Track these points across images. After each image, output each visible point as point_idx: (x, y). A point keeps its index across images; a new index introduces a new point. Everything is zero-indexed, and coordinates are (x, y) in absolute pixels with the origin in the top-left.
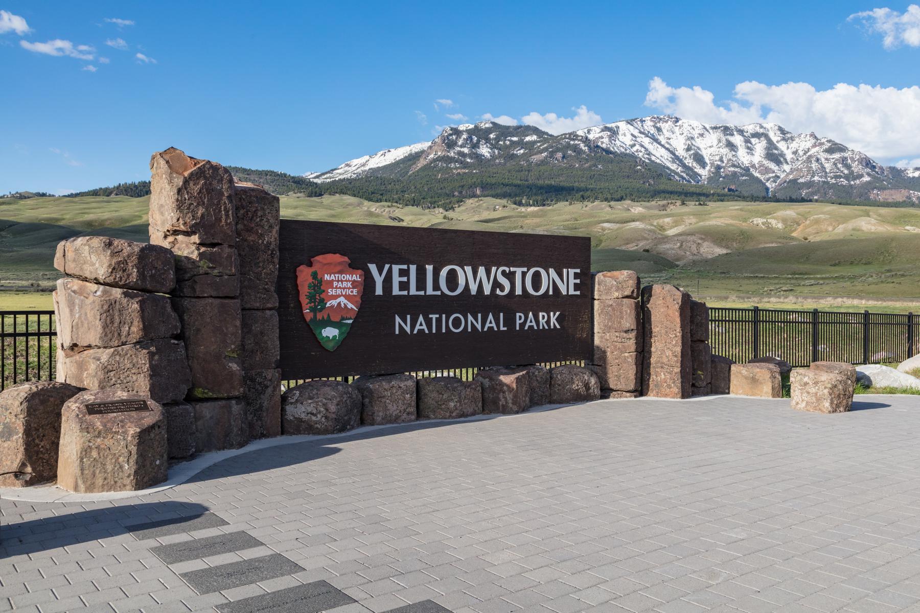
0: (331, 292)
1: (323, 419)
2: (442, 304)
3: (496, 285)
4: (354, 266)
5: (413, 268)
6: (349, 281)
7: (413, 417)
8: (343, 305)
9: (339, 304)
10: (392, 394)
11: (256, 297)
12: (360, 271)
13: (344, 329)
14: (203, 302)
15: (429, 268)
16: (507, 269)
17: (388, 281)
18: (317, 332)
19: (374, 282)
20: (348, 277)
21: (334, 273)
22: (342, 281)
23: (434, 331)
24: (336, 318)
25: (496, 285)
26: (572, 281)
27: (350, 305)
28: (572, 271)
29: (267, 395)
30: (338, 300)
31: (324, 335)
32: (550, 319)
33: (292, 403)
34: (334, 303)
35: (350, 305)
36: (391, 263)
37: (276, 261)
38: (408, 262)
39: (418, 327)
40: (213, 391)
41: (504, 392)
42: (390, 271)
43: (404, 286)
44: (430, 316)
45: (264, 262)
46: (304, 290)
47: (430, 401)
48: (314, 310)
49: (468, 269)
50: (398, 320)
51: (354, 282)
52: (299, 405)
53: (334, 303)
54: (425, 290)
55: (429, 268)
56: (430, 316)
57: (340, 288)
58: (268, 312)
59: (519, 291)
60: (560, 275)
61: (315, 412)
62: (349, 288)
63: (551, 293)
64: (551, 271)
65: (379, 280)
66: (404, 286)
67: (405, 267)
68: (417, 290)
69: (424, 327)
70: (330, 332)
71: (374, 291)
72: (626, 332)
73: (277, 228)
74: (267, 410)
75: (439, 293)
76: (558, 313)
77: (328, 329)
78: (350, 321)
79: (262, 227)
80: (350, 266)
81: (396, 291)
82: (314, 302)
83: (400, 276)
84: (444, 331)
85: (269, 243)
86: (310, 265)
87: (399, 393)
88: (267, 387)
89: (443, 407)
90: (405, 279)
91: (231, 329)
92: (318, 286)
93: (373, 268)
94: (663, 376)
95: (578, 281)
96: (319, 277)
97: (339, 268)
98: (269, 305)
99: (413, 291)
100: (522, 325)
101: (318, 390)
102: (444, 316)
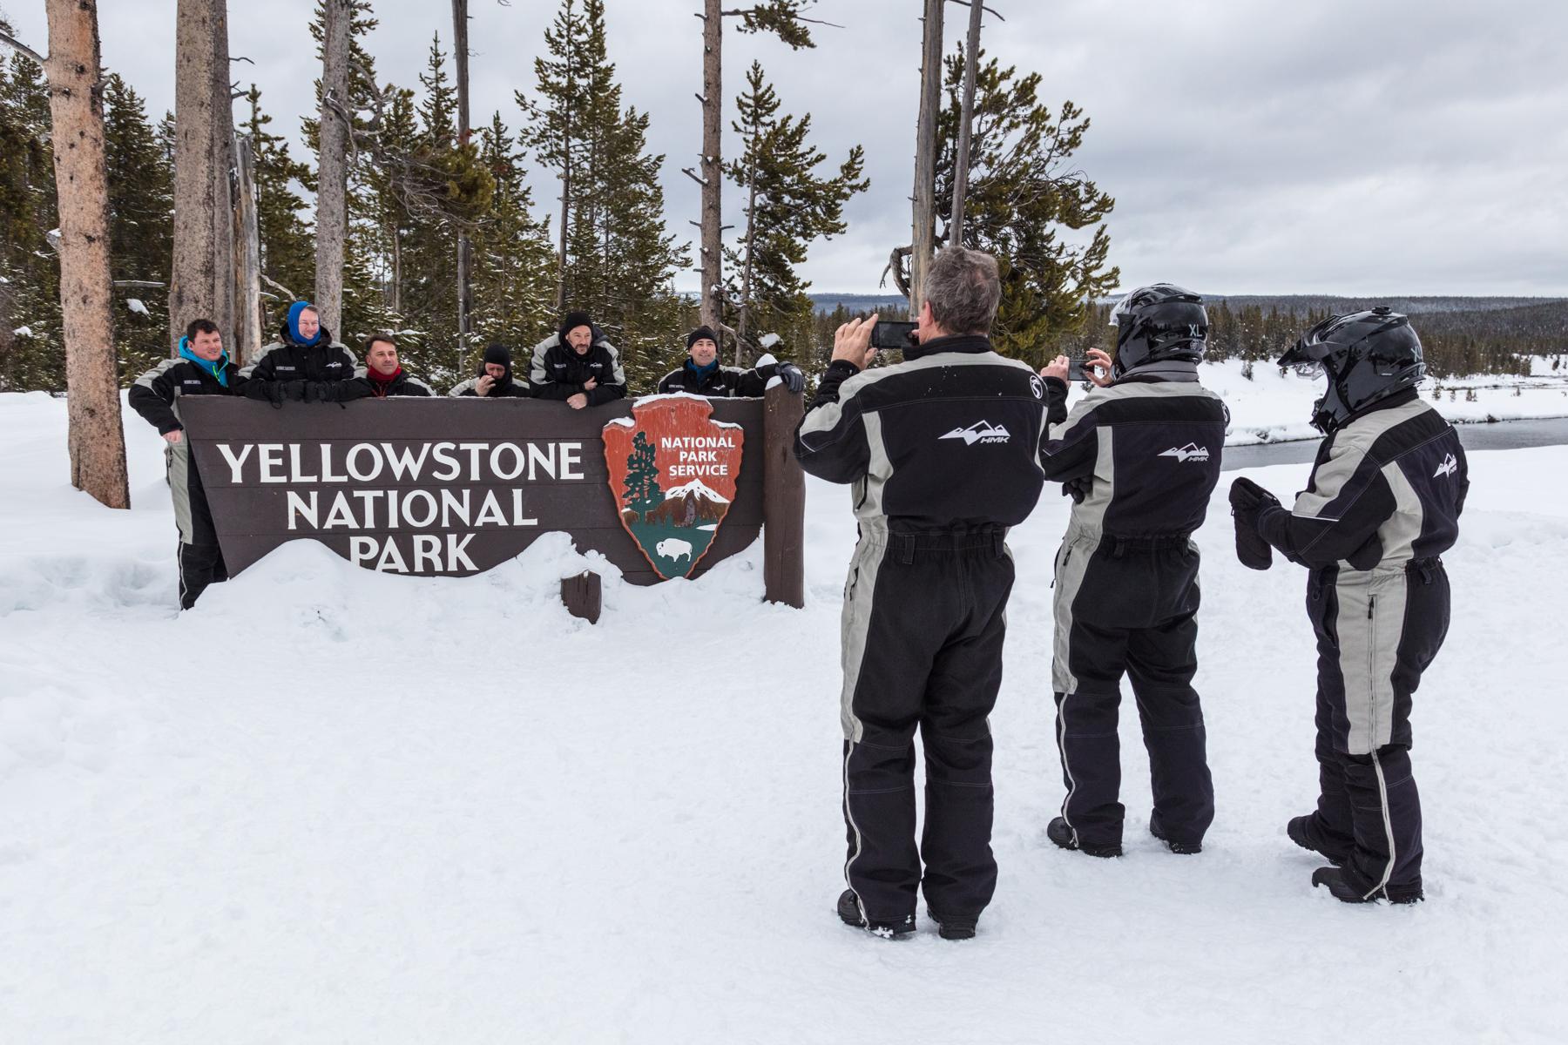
5: (295, 449)
16: (452, 446)
17: (252, 466)
36: (256, 441)
42: (254, 454)
49: (388, 447)
54: (320, 477)
63: (532, 477)
64: (532, 447)
65: (236, 466)
67: (280, 447)
81: (266, 477)
90: (279, 462)
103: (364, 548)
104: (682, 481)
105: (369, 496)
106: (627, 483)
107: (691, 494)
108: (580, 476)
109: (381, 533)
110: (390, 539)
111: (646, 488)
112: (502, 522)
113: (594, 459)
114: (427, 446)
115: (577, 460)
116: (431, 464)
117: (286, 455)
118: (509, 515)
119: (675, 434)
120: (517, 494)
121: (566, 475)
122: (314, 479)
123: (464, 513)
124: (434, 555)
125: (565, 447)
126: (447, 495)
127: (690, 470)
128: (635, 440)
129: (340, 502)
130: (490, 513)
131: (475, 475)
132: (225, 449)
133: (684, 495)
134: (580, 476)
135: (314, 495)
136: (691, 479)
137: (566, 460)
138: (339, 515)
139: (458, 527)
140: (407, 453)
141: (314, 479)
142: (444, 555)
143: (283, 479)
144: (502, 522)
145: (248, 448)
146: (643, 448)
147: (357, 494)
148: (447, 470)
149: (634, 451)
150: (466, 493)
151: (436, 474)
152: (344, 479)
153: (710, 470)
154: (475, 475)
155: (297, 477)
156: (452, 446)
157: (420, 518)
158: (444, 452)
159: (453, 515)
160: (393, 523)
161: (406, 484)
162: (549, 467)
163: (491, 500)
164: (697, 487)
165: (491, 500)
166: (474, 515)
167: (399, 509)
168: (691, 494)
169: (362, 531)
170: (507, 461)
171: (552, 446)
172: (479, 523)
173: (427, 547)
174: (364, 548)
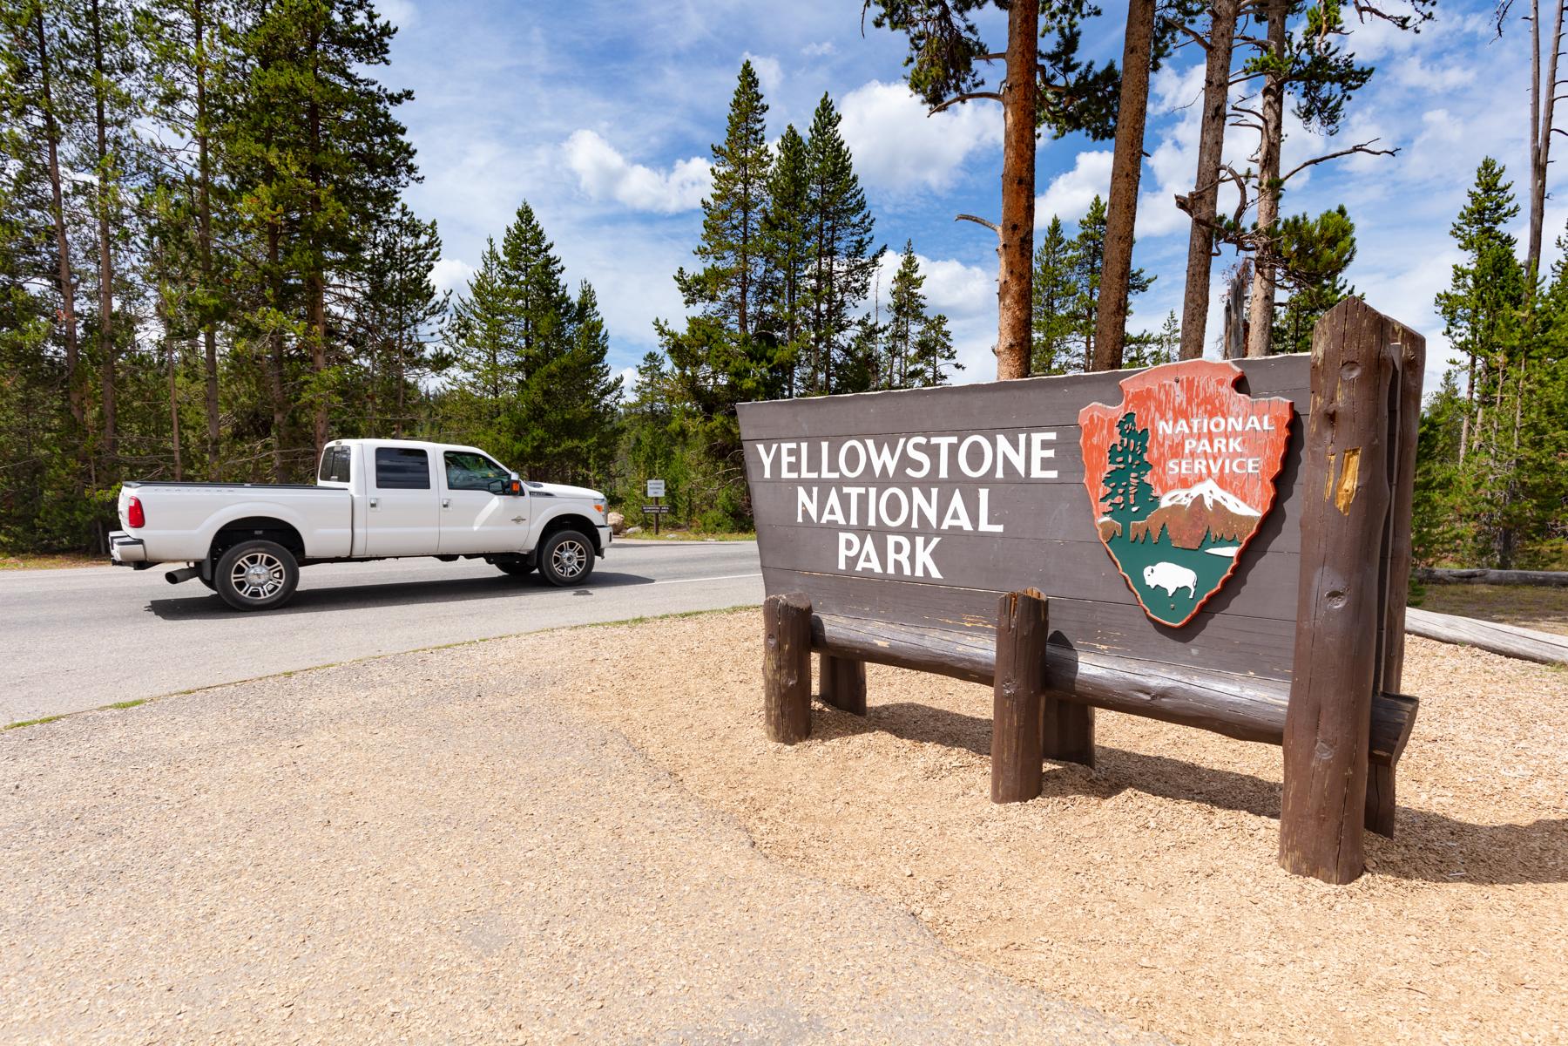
5: (804, 446)
16: (923, 440)
36: (780, 440)
49: (870, 443)
63: (1000, 474)
64: (1001, 439)
65: (767, 462)
66: (795, 467)
67: (794, 445)
81: (785, 474)
90: (793, 459)
103: (849, 545)
104: (1185, 483)
105: (854, 492)
106: (1106, 481)
107: (1199, 500)
108: (1053, 474)
109: (862, 530)
110: (869, 538)
111: (1132, 490)
112: (968, 527)
113: (1067, 453)
114: (902, 441)
115: (1050, 453)
116: (905, 461)
117: (795, 452)
118: (974, 519)
119: (1181, 414)
120: (984, 494)
121: (1037, 472)
122: (815, 475)
123: (931, 514)
124: (903, 558)
125: (1037, 438)
126: (916, 491)
127: (1200, 466)
128: (1120, 424)
129: (833, 499)
130: (955, 516)
131: (943, 473)
132: (761, 447)
133: (1188, 502)
134: (1053, 474)
135: (815, 490)
136: (1201, 479)
137: (1038, 454)
138: (832, 512)
139: (925, 529)
140: (886, 448)
141: (815, 475)
142: (912, 558)
143: (794, 475)
144: (968, 527)
145: (775, 446)
146: (1131, 434)
147: (846, 490)
148: (918, 466)
149: (1117, 439)
150: (934, 491)
151: (909, 471)
152: (836, 475)
153: (1232, 467)
154: (943, 473)
155: (805, 474)
156: (923, 440)
157: (893, 518)
158: (917, 447)
159: (922, 517)
160: (872, 522)
161: (883, 482)
162: (1019, 462)
163: (957, 501)
164: (1210, 492)
165: (957, 501)
166: (940, 519)
167: (877, 509)
168: (1201, 497)
169: (847, 529)
170: (975, 456)
171: (1022, 437)
172: (945, 526)
173: (899, 548)
174: (849, 545)
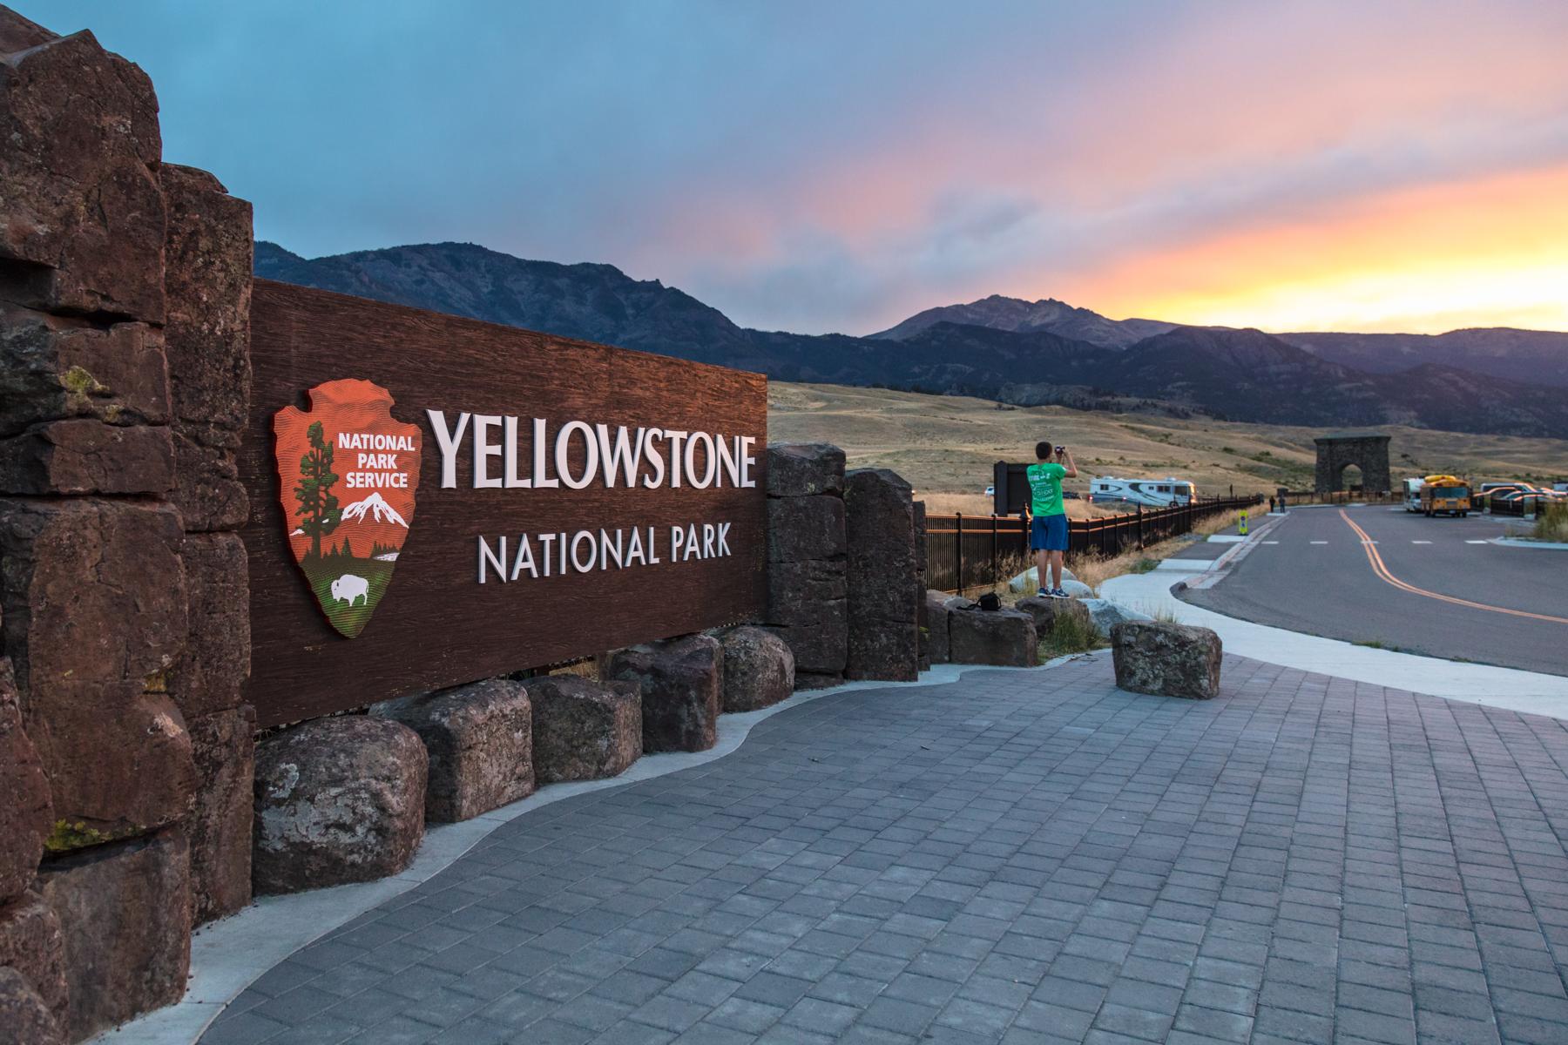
0: (353, 480)
1: (371, 839)
2: (557, 510)
3: (646, 467)
4: (408, 412)
5: (512, 423)
6: (391, 452)
7: (528, 786)
8: (377, 516)
9: (370, 511)
10: (490, 734)
11: (192, 494)
12: (414, 426)
13: (380, 578)
14: (66, 512)
15: (540, 425)
16: (659, 432)
17: (466, 453)
18: (318, 590)
19: (439, 455)
20: (389, 442)
21: (360, 432)
22: (376, 452)
23: (547, 574)
24: (361, 551)
25: (646, 467)
26: (748, 461)
27: (393, 516)
28: (746, 440)
29: (219, 791)
30: (367, 503)
31: (337, 596)
32: (708, 542)
33: (279, 802)
34: (356, 509)
35: (393, 516)
36: (474, 410)
37: (246, 386)
38: (503, 412)
39: (520, 565)
40: (101, 822)
41: (689, 703)
43: (496, 466)
44: (542, 537)
45: (216, 389)
46: (293, 476)
47: (554, 741)
48: (313, 529)
49: (603, 429)
50: (485, 548)
51: (401, 454)
52: (302, 805)
53: (356, 509)
55: (540, 425)
56: (542, 537)
57: (372, 470)
58: (221, 538)
59: (676, 483)
60: (731, 447)
61: (348, 818)
62: (391, 471)
64: (720, 437)
67: (497, 421)
68: (519, 478)
69: (531, 564)
70: (350, 588)
71: (440, 478)
72: (833, 558)
73: (247, 293)
74: (218, 834)
75: (554, 483)
76: (728, 525)
77: (347, 579)
78: (392, 557)
79: (211, 284)
80: (393, 411)
81: (481, 481)
82: (315, 508)
83: (490, 442)
84: (563, 571)
85: (229, 335)
86: (306, 404)
87: (503, 729)
88: (218, 765)
89: (583, 750)
90: (496, 450)
91: (163, 602)
92: (326, 465)
93: (437, 418)
94: (884, 640)
95: (752, 461)
96: (326, 439)
97: (369, 418)
98: (228, 519)
99: (512, 481)
100: (681, 550)
101: (350, 754)
102: (564, 535)
